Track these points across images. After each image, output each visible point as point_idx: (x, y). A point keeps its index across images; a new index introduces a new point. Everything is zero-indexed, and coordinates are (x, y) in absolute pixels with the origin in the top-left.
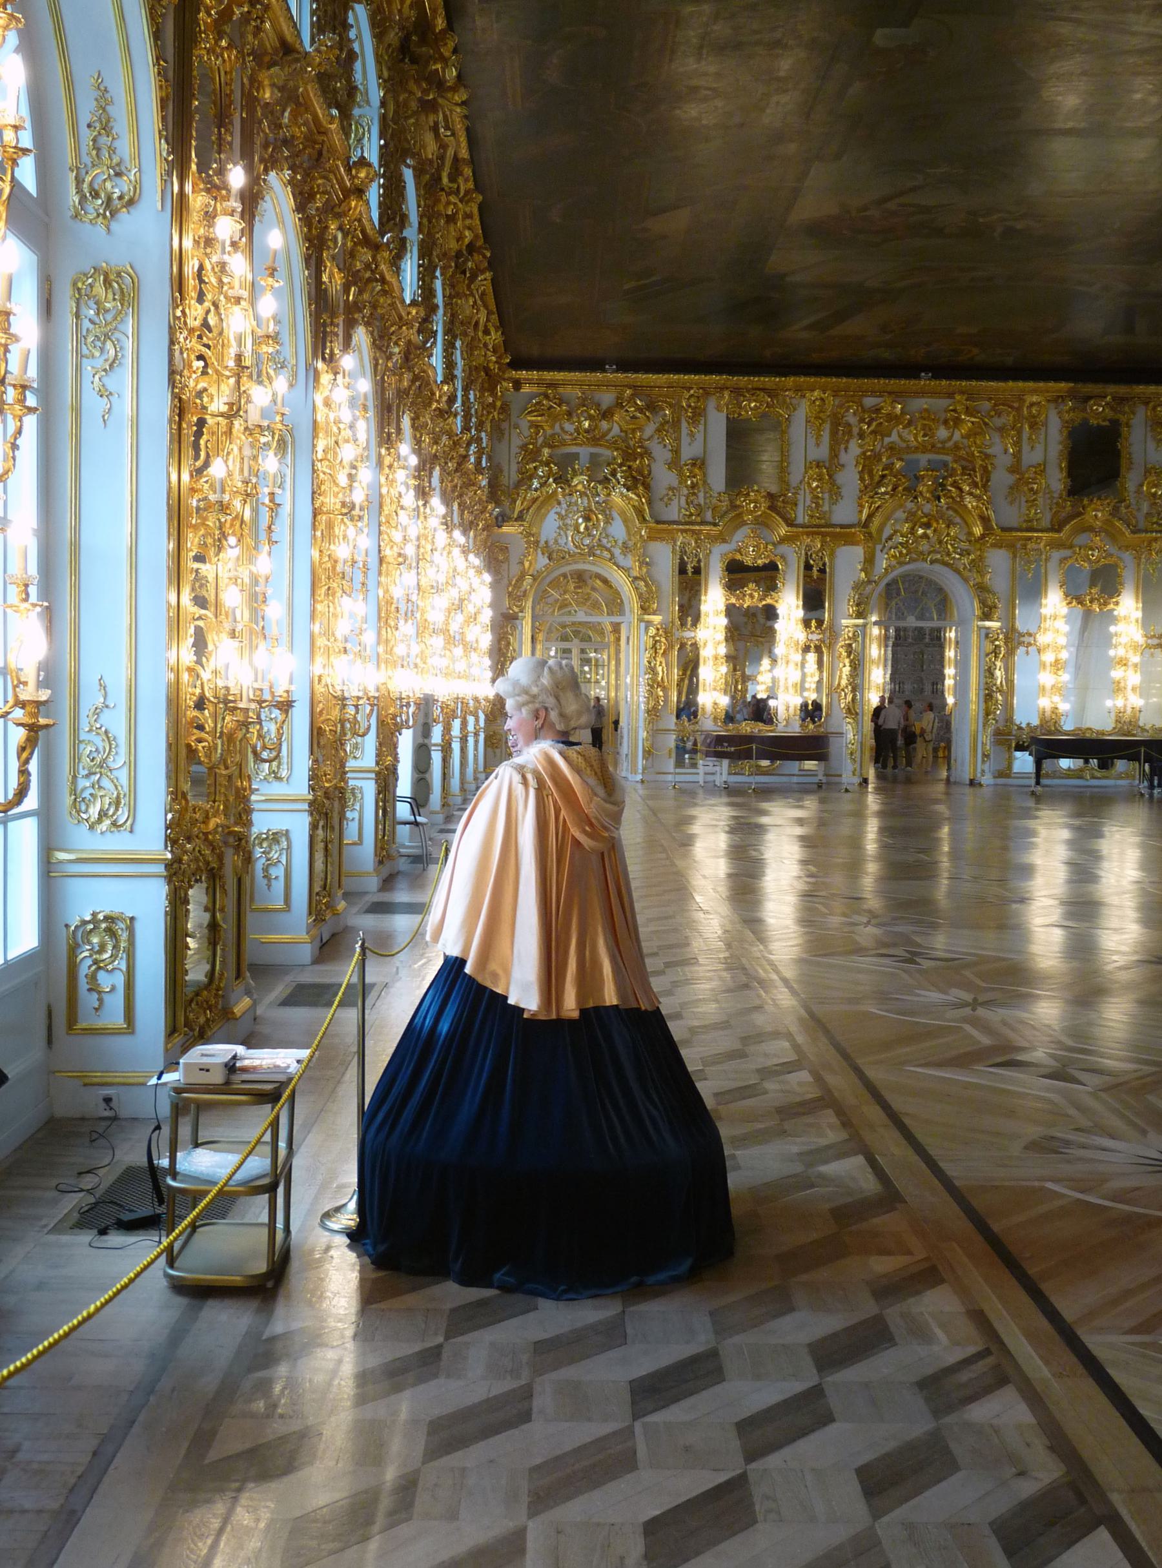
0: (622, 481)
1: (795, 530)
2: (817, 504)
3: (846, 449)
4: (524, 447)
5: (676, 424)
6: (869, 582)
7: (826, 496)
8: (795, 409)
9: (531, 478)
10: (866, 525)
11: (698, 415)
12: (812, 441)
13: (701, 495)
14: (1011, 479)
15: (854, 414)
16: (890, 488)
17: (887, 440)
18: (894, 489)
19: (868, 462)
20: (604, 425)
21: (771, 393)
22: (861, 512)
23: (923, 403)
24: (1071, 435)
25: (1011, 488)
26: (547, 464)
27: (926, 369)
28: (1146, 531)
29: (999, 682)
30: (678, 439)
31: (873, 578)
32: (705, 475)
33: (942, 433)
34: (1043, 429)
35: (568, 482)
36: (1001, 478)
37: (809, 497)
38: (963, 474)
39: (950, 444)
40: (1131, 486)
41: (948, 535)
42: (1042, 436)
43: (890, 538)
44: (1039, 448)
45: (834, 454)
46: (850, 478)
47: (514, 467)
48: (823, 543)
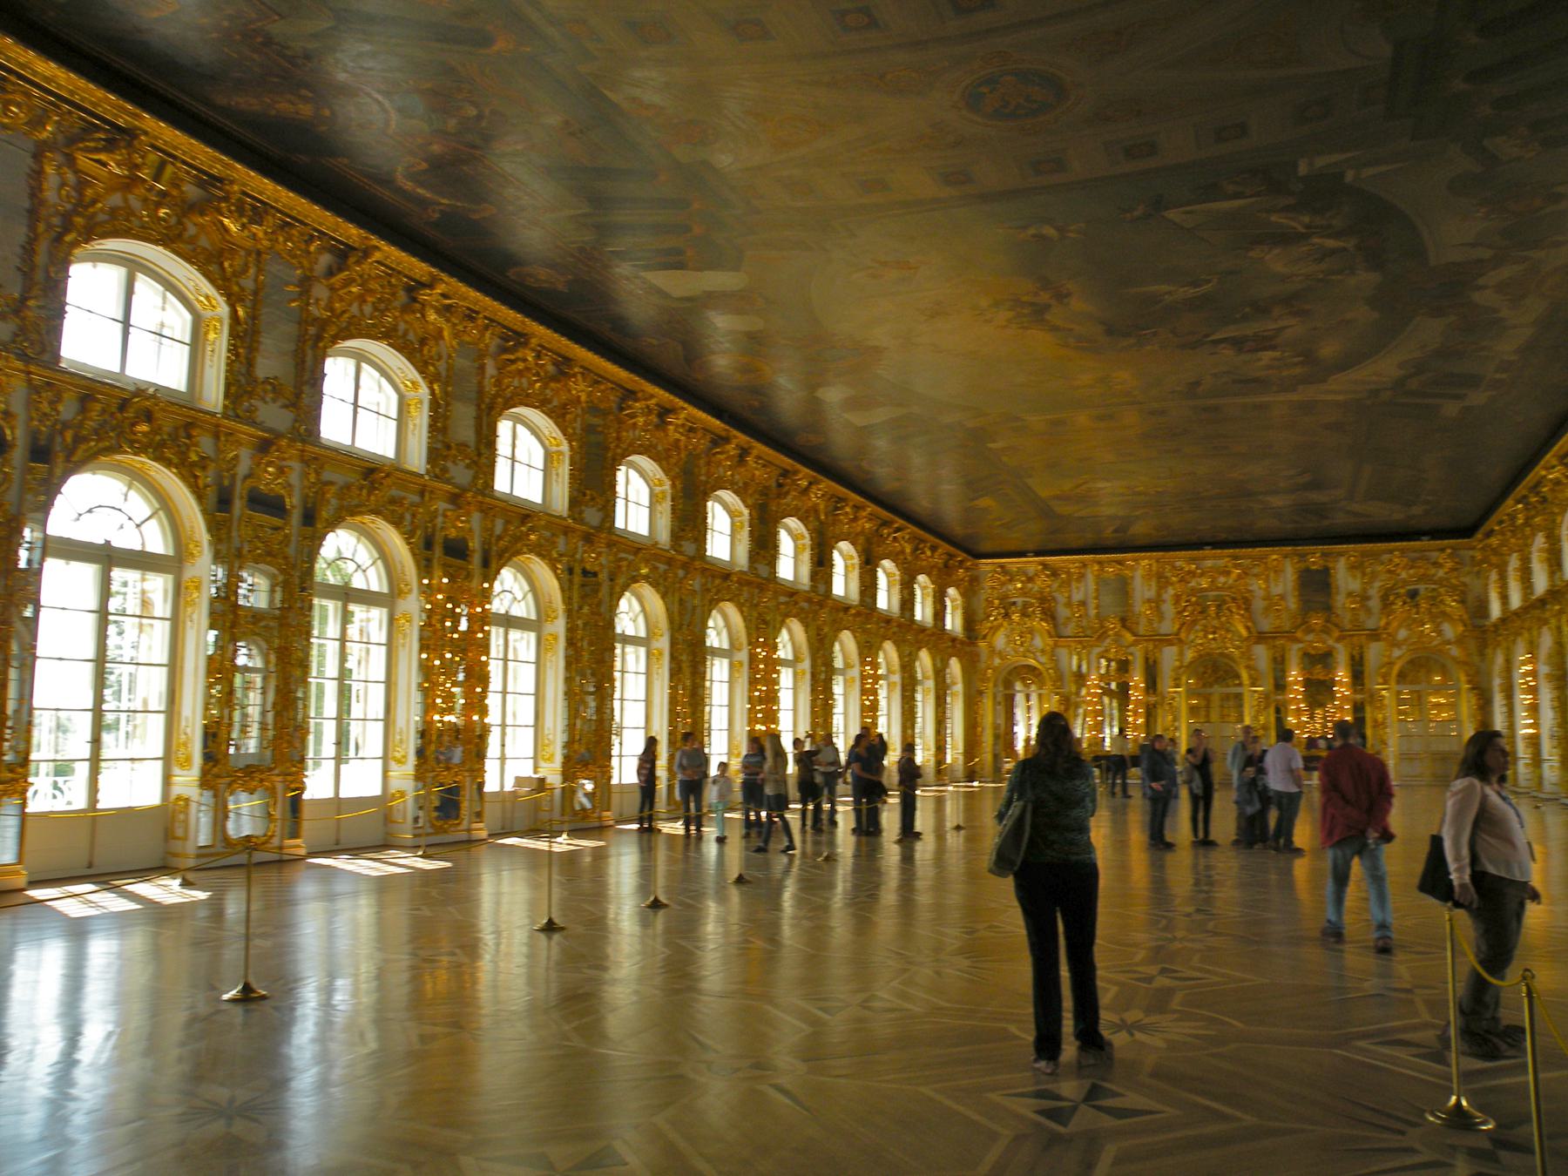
5: (1069, 585)
10: (1177, 634)
11: (1082, 576)
19: (1177, 598)
21: (1119, 562)
24: (1300, 577)
27: (1208, 544)
33: (1222, 579)
36: (1259, 604)
40: (1339, 605)
45: (1159, 595)
46: (1169, 609)
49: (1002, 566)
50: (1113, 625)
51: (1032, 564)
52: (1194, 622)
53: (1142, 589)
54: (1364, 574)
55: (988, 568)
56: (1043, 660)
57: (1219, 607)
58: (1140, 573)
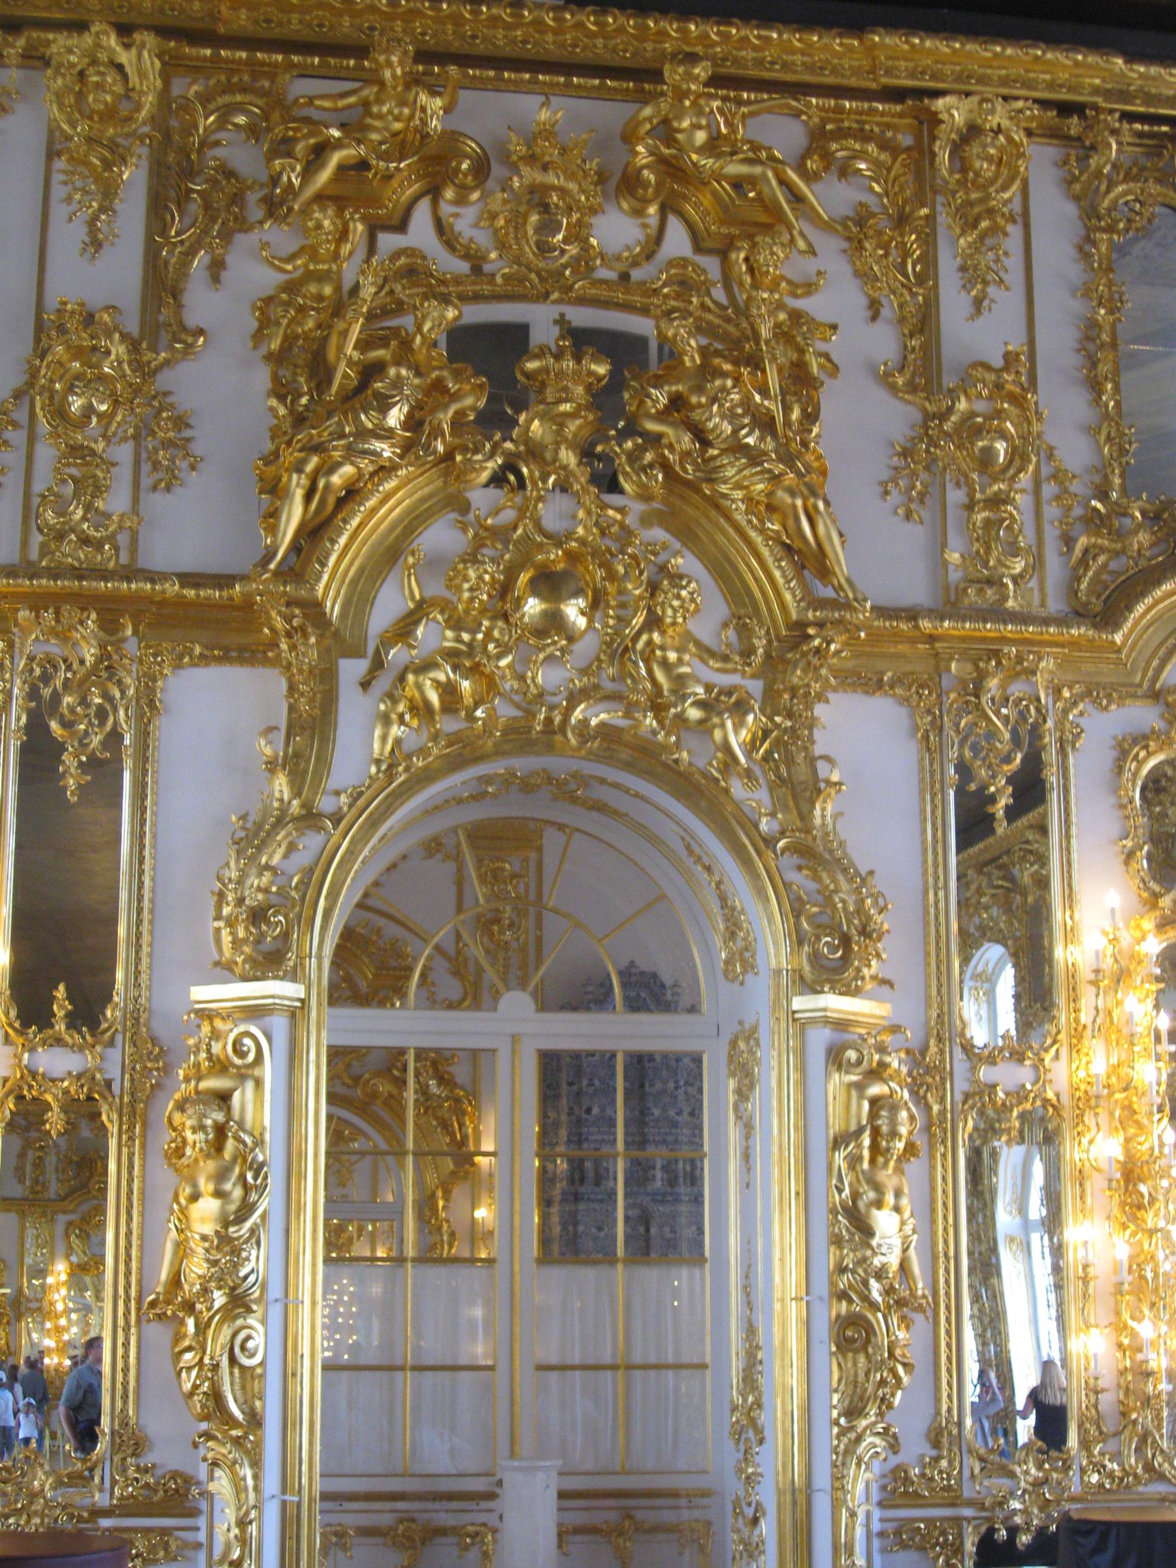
3: (217, 267)
6: (310, 818)
7: (124, 453)
12: (68, 235)
14: (896, 417)
15: (253, 131)
16: (395, 417)
17: (388, 241)
18: (413, 423)
22: (272, 516)
23: (541, 109)
25: (905, 453)
29: (893, 1261)
31: (325, 804)
33: (616, 230)
34: (1015, 231)
37: (46, 454)
38: (707, 371)
41: (654, 622)
42: (1014, 264)
43: (404, 630)
44: (1006, 303)
45: (162, 285)
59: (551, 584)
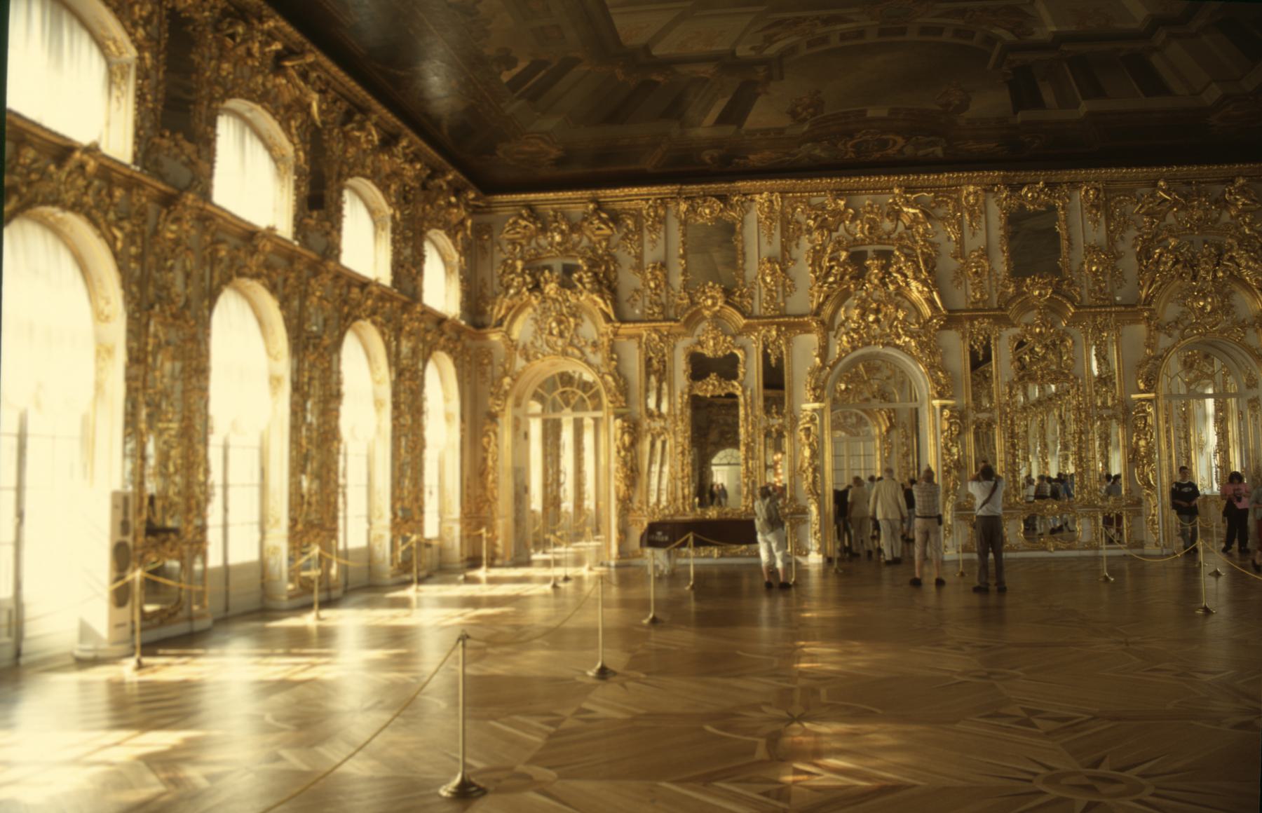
0: (588, 286)
1: (751, 321)
2: (772, 297)
3: (797, 245)
4: (504, 262)
7: (780, 289)
8: (747, 212)
9: (508, 288)
10: (817, 313)
12: (764, 240)
13: (663, 294)
17: (835, 235)
19: (817, 255)
20: (575, 237)
21: (723, 198)
26: (522, 274)
28: (1090, 307)
30: (641, 245)
32: (666, 276)
33: (887, 225)
35: (542, 292)
36: (948, 264)
37: (764, 291)
39: (894, 236)
41: (896, 318)
44: (982, 235)
45: (785, 248)
47: (496, 281)
48: (778, 330)
49: (530, 207)
50: (711, 301)
51: (575, 202)
52: (846, 295)
53: (757, 241)
54: (1109, 217)
55: (509, 211)
56: (597, 359)
57: (885, 269)
58: (755, 214)
59: (877, 311)
